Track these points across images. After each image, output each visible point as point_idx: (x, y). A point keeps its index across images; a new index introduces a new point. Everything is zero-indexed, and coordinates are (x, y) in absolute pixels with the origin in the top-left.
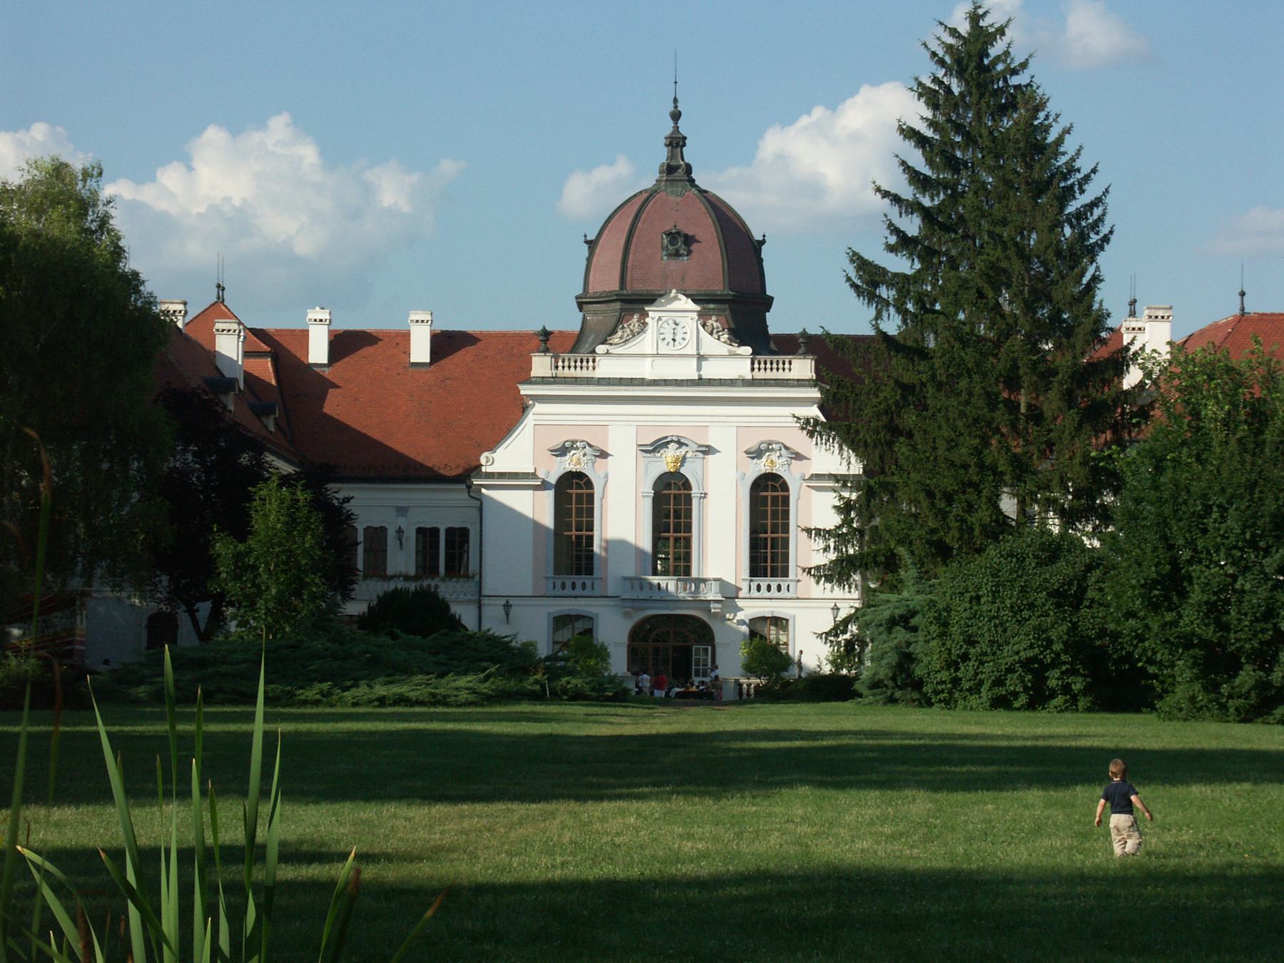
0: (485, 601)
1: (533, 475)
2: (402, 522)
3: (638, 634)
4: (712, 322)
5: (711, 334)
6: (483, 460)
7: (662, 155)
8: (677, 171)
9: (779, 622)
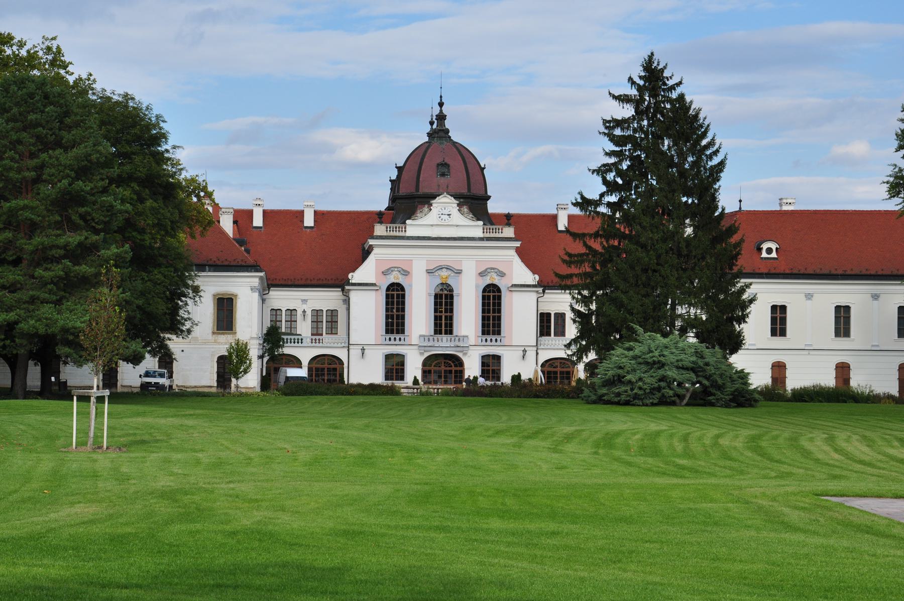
0: (351, 347)
2: (305, 307)
3: (425, 363)
4: (465, 209)
6: (350, 276)
8: (439, 131)
9: (497, 358)
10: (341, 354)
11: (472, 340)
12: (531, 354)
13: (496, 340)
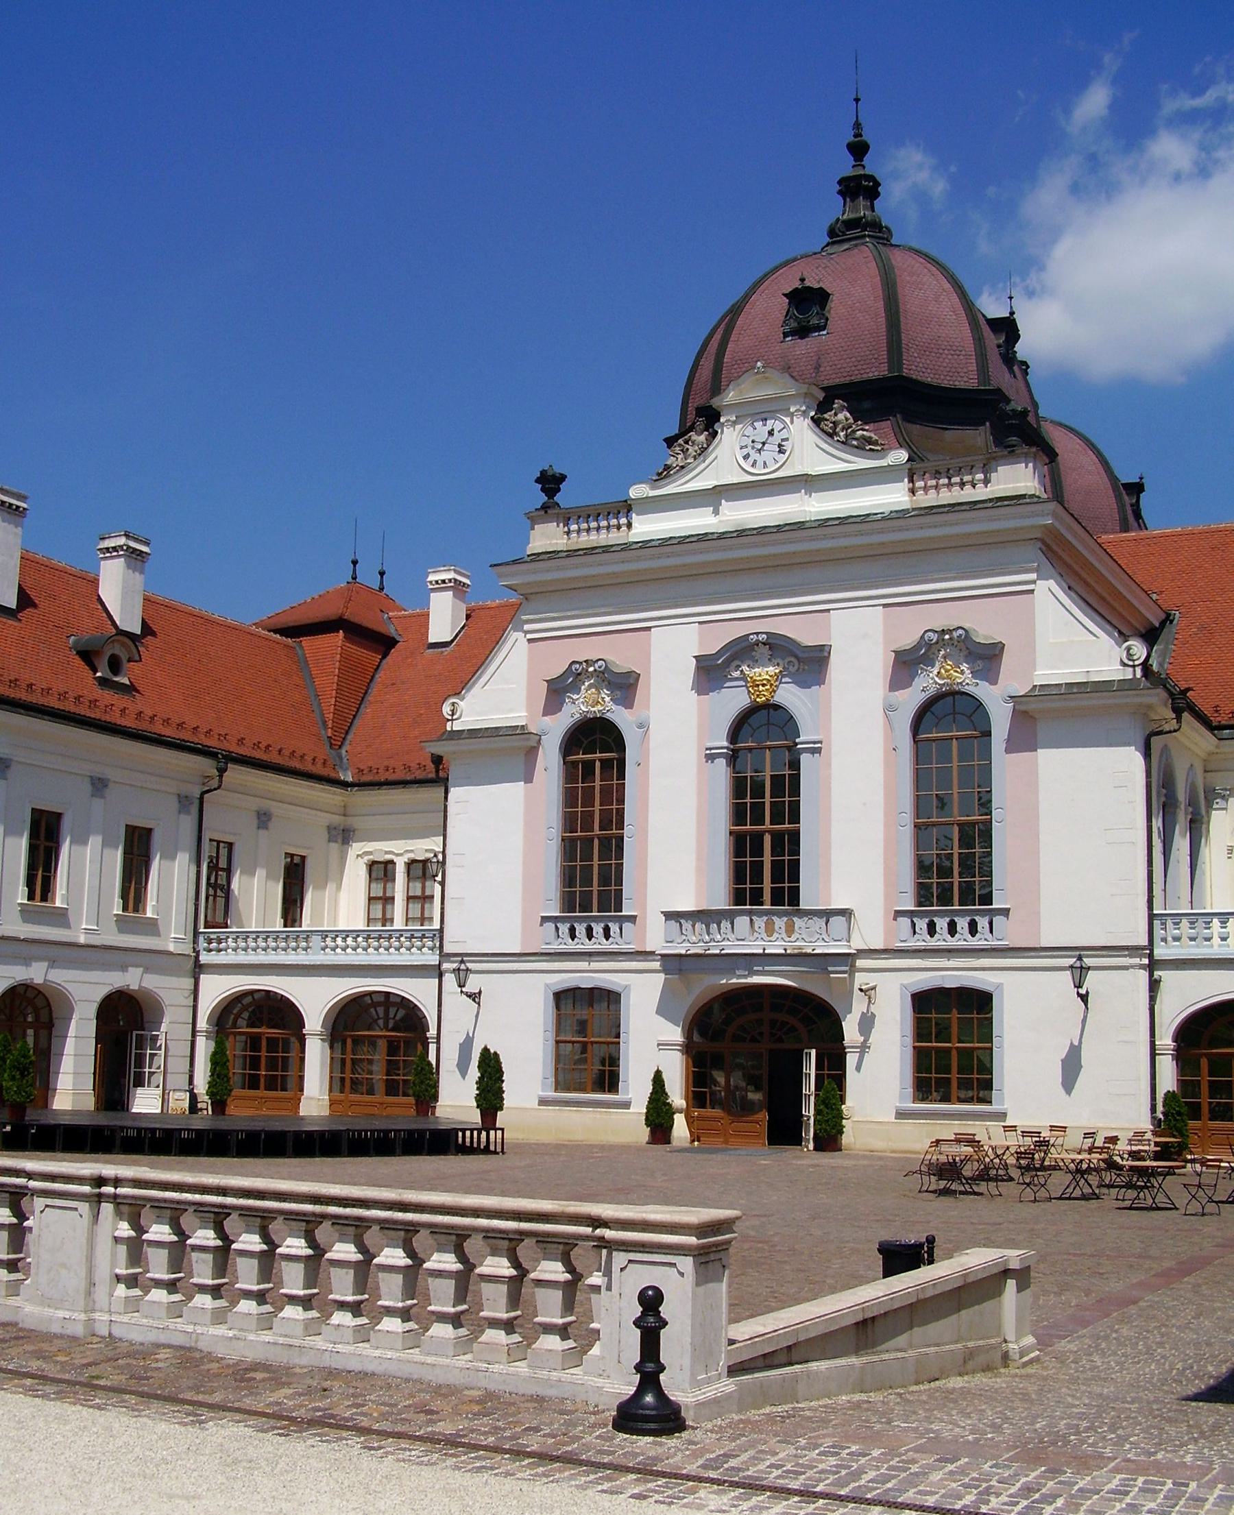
6: (446, 709)
7: (835, 209)
10: (419, 991)
11: (871, 930)
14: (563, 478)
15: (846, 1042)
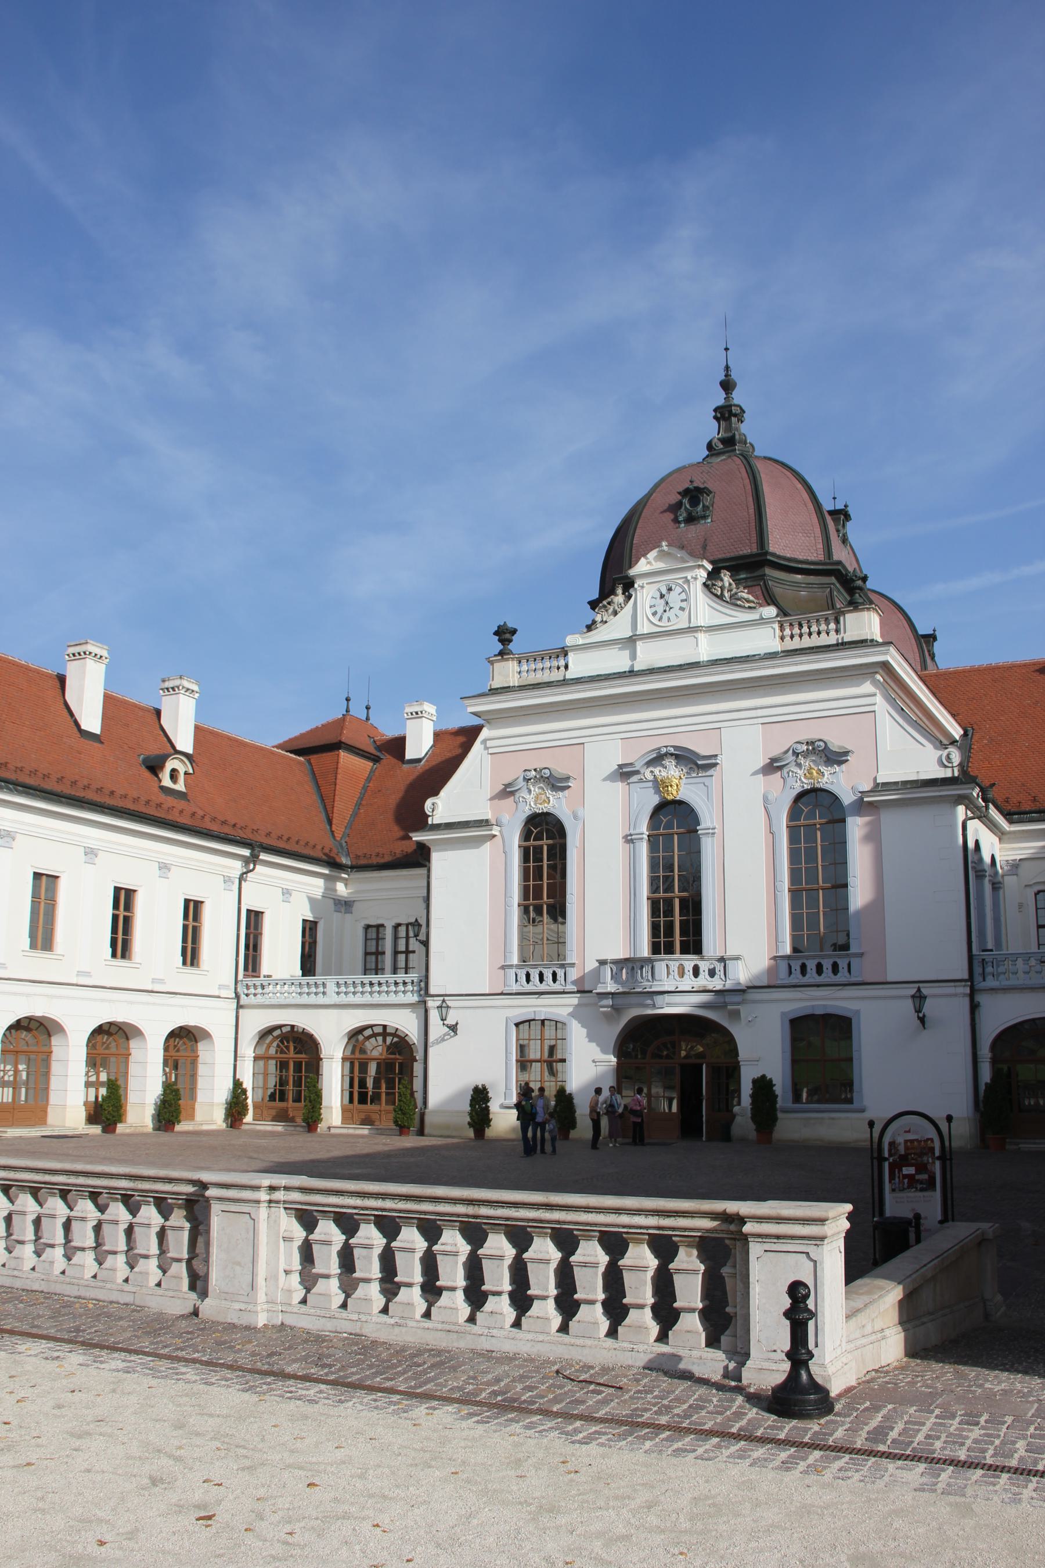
1: (484, 823)
5: (721, 597)
7: (711, 430)
9: (839, 1027)
12: (949, 1009)
13: (835, 968)
14: (514, 632)
15: (740, 1059)
